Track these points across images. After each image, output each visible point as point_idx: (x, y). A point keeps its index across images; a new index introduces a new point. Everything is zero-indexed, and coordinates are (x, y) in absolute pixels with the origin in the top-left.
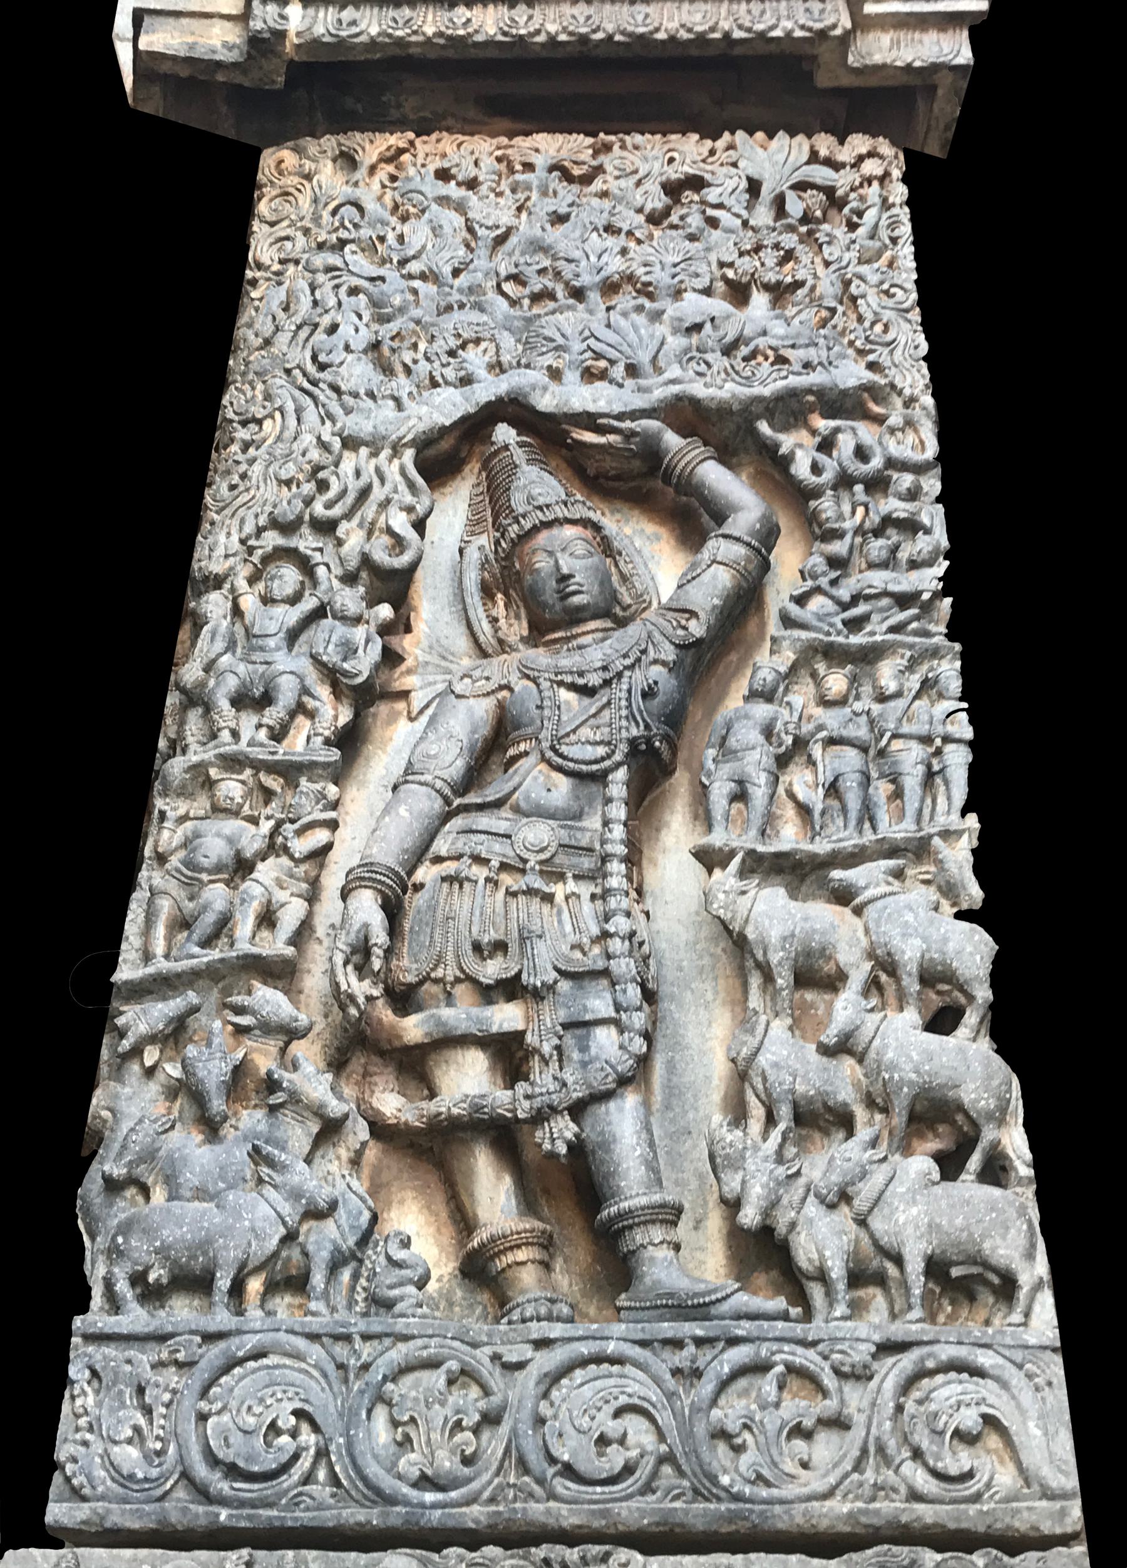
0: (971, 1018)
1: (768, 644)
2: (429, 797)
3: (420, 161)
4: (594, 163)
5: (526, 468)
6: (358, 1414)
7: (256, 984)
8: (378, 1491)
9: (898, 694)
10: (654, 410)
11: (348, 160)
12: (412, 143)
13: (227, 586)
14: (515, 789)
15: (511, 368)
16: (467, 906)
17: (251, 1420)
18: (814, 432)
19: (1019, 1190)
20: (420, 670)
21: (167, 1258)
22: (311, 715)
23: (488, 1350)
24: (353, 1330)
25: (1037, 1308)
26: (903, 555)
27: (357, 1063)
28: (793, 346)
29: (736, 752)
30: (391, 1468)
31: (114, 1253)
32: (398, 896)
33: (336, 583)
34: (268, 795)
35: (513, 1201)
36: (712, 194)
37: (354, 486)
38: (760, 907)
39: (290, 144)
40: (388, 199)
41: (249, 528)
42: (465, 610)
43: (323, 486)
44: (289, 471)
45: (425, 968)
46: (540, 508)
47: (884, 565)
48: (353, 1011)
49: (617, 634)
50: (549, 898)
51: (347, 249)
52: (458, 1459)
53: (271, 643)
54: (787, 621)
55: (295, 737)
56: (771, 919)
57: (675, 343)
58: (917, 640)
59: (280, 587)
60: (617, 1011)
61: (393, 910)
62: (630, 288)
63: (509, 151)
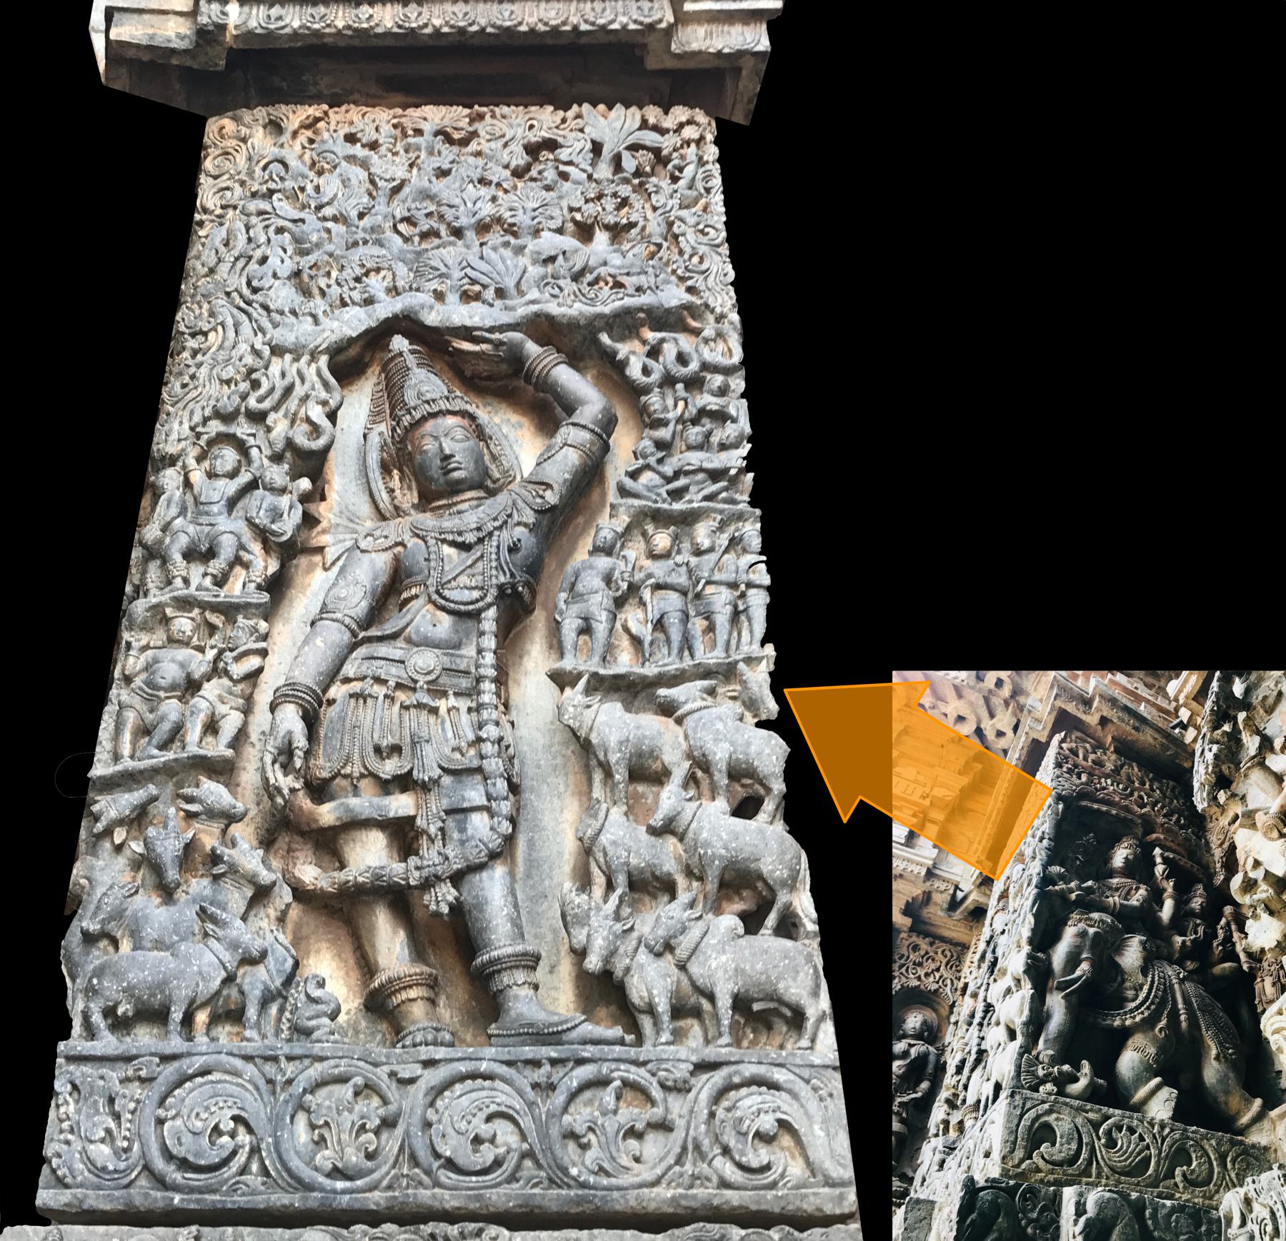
1: (608, 510)
2: (340, 631)
3: (332, 127)
4: (471, 129)
5: (416, 370)
6: (283, 1119)
9: (711, 550)
11: (275, 127)
12: (326, 113)
14: (408, 625)
15: (405, 291)
16: (369, 718)
17: (199, 1124)
18: (644, 342)
20: (333, 530)
23: (386, 1069)
24: (279, 1052)
26: (715, 439)
28: (628, 274)
29: (582, 595)
32: (315, 709)
33: (266, 461)
35: (406, 951)
36: (564, 154)
37: (280, 385)
38: (602, 718)
39: (230, 114)
40: (307, 157)
42: (368, 483)
43: (256, 385)
44: (229, 372)
45: (337, 766)
46: (428, 402)
47: (700, 447)
49: (489, 502)
50: (434, 711)
51: (275, 197)
54: (623, 492)
55: (233, 583)
56: (610, 727)
57: (535, 271)
58: (726, 506)
59: (222, 464)
60: (489, 800)
61: (311, 721)
62: (499, 228)
63: (403, 120)
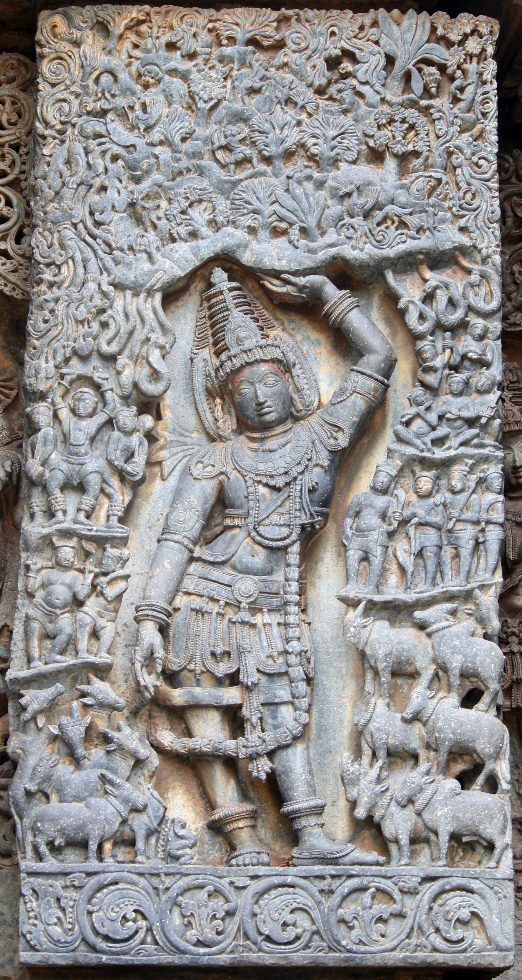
0: (486, 699)
4: (277, 37)
6: (166, 912)
7: (94, 679)
8: (177, 948)
9: (462, 491)
10: (318, 268)
12: (148, 14)
13: (50, 400)
15: (224, 226)
19: (502, 796)
20: (168, 446)
21: (64, 834)
22: (109, 496)
23: (227, 880)
25: (504, 858)
27: (144, 711)
30: (182, 936)
31: (35, 830)
34: (88, 554)
36: (361, 71)
37: (125, 328)
38: (374, 636)
39: (61, 9)
40: (134, 69)
41: (60, 358)
44: (82, 313)
45: (183, 663)
48: (147, 695)
52: (214, 933)
53: (82, 450)
55: (99, 511)
59: (84, 407)
63: (218, 25)
